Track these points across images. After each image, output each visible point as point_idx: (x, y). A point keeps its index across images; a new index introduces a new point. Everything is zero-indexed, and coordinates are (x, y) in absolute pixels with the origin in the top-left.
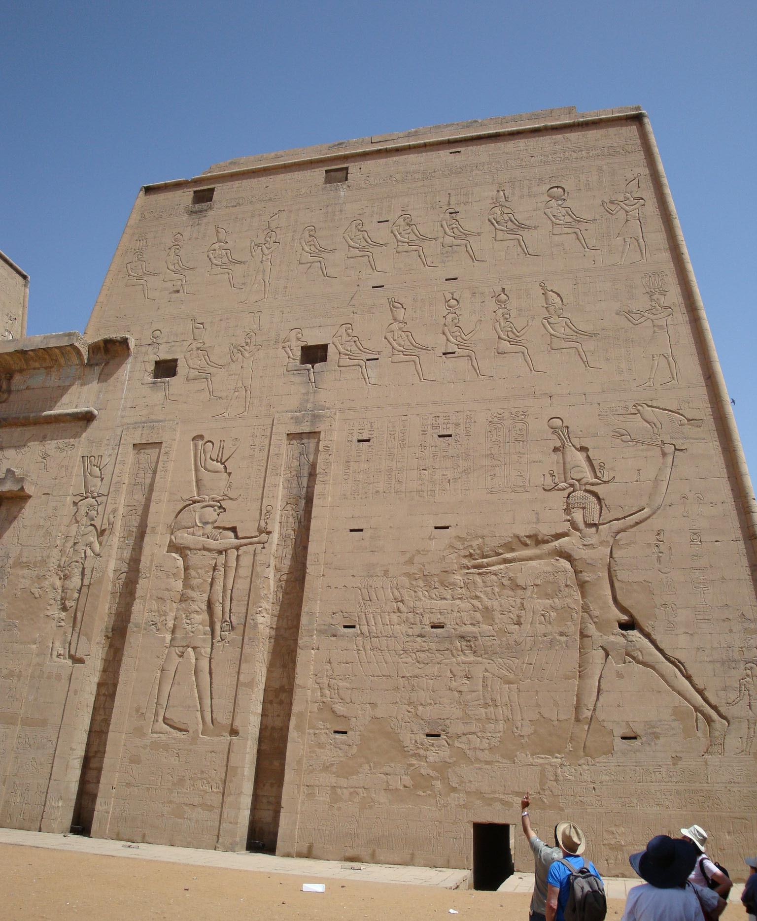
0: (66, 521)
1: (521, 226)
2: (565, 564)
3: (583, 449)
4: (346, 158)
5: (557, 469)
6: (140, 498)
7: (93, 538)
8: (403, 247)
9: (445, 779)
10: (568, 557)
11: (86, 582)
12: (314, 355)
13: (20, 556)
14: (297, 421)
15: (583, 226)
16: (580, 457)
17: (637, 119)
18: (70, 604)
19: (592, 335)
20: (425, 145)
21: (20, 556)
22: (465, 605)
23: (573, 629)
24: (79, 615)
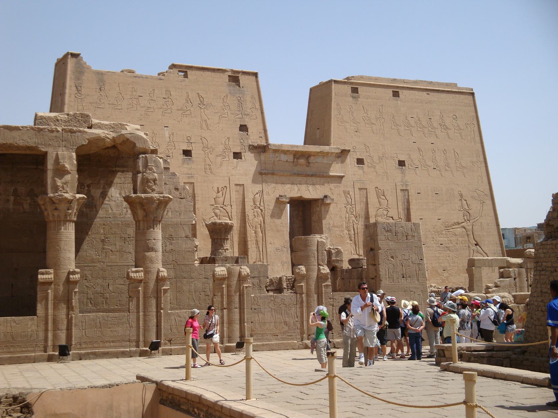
0: (345, 212)
1: (447, 128)
2: (464, 229)
3: (465, 200)
4: (398, 87)
5: (461, 205)
6: (363, 206)
7: (354, 219)
8: (419, 129)
9: (448, 280)
10: (465, 228)
11: (356, 232)
12: (402, 163)
13: (334, 224)
14: (402, 185)
15: (461, 131)
16: (465, 202)
17: (473, 94)
18: (353, 239)
19: (465, 168)
20: (420, 89)
21: (334, 224)
22: (446, 239)
23: (467, 246)
24: (357, 242)
